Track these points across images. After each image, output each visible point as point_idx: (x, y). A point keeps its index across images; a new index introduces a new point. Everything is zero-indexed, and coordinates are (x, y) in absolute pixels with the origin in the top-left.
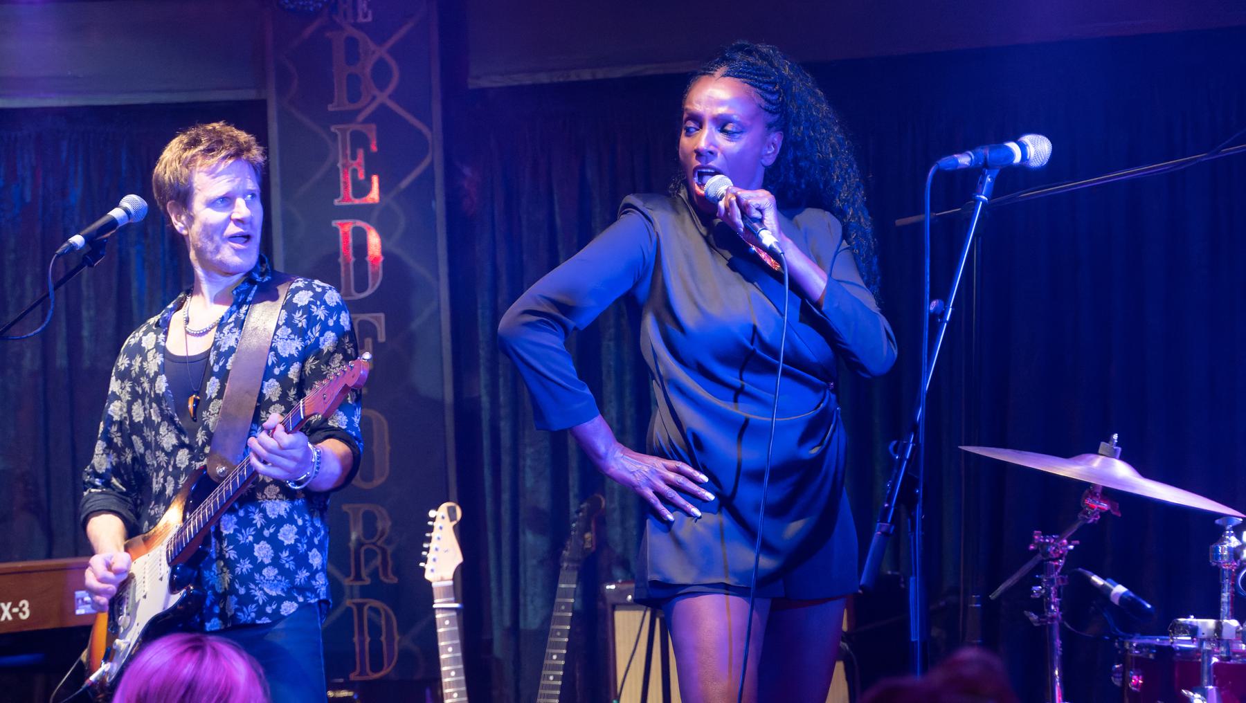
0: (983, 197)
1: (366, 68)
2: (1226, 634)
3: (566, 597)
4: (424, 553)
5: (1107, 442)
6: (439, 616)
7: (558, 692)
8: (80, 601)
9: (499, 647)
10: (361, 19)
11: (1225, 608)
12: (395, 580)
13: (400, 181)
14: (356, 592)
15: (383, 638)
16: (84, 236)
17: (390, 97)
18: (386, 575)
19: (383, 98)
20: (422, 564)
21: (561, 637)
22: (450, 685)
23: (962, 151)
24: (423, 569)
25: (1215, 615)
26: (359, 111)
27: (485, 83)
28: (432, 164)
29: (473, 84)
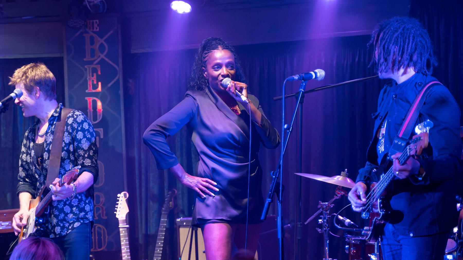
1: (97, 46)
3: (163, 223)
6: (121, 230)
7: (161, 255)
9: (141, 241)
10: (95, 30)
13: (108, 84)
15: (102, 237)
18: (103, 216)
19: (102, 56)
20: (115, 212)
22: (124, 253)
24: (116, 214)
26: (95, 61)
28: (119, 79)
29: (133, 51)
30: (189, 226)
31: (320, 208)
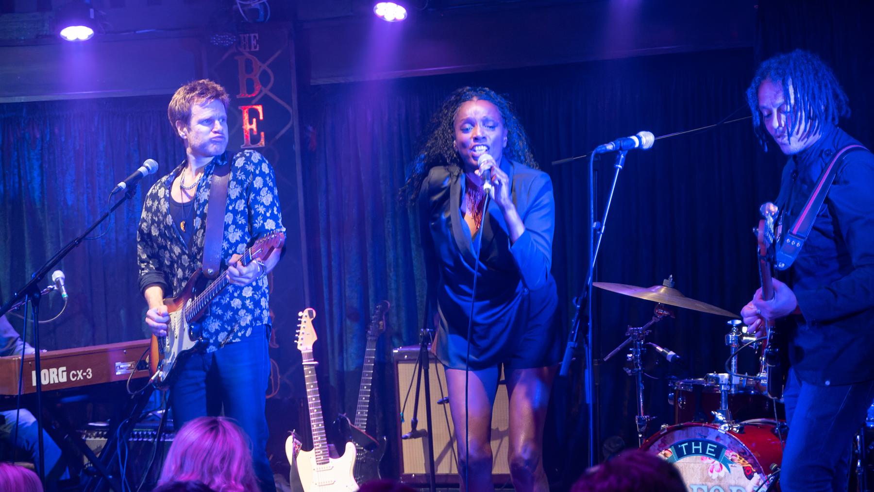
1: (256, 76)
4: (297, 335)
5: (667, 279)
6: (305, 369)
8: (118, 368)
9: (333, 382)
10: (253, 49)
11: (734, 368)
12: (277, 346)
16: (125, 183)
20: (296, 341)
21: (368, 376)
22: (312, 405)
23: (608, 142)
24: (296, 344)
26: (253, 98)
27: (321, 82)
28: (292, 128)
29: (313, 82)
30: (415, 360)
31: (629, 336)
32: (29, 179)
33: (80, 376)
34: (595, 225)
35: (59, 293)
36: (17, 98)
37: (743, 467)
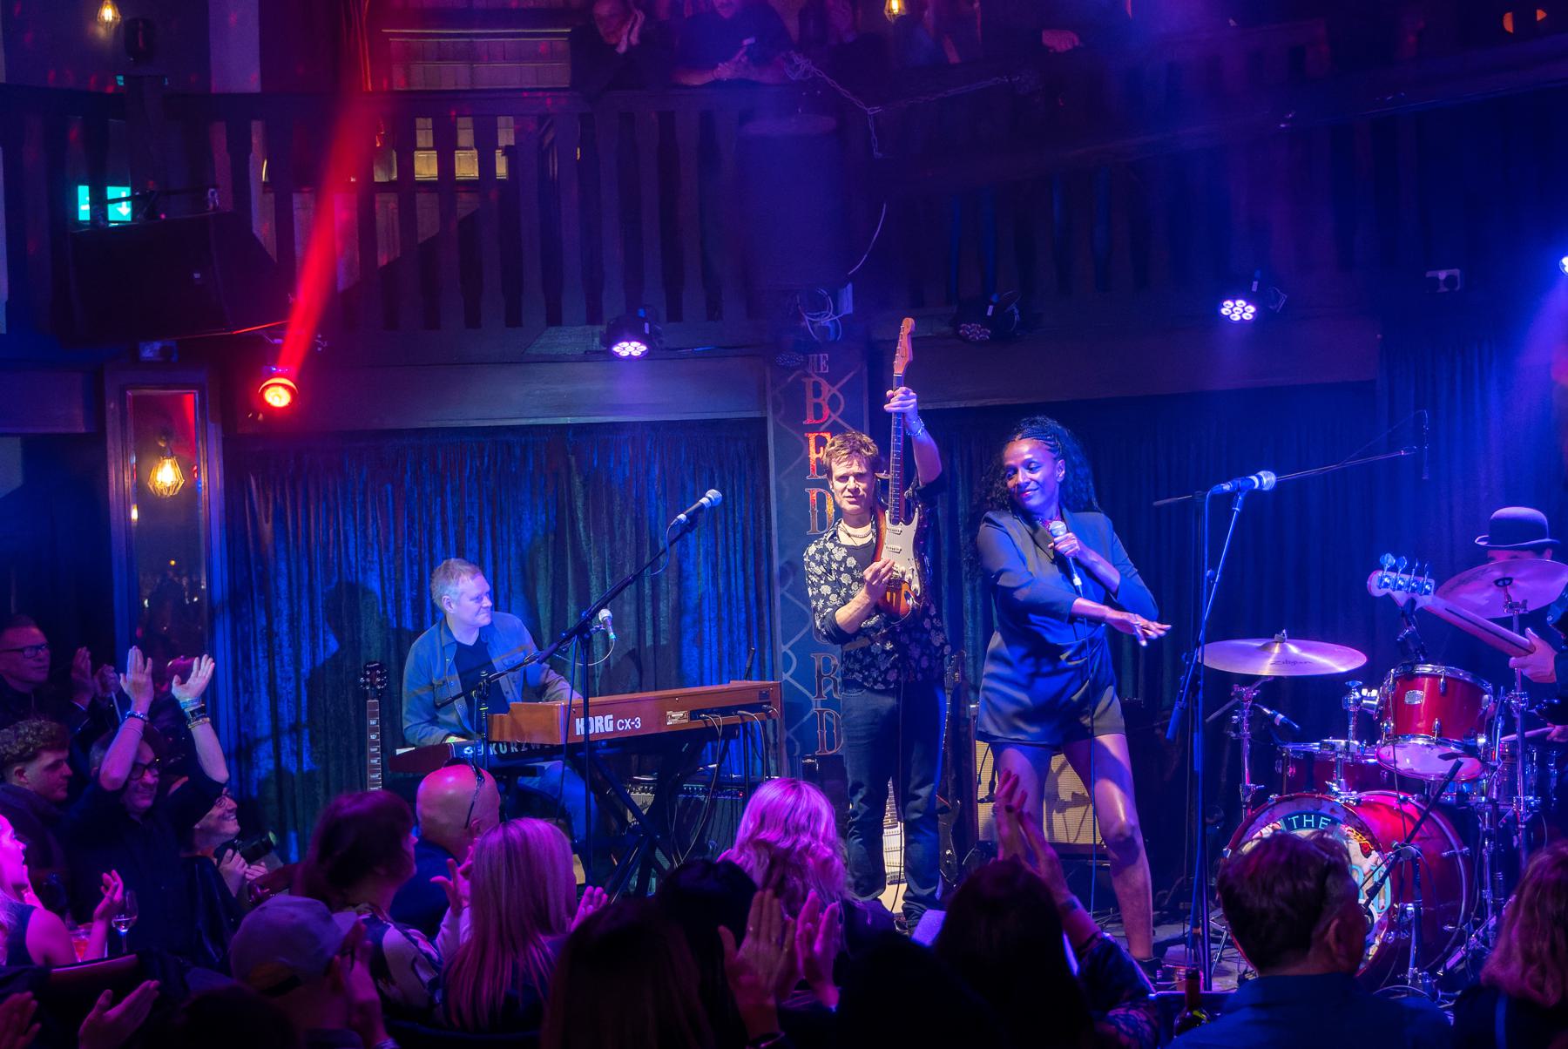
0: (1237, 509)
2: (1352, 750)
10: (822, 371)
11: (1351, 734)
14: (819, 704)
17: (839, 416)
19: (835, 417)
25: (1345, 736)
26: (820, 425)
32: (574, 507)
33: (628, 725)
34: (1208, 573)
35: (606, 635)
36: (562, 419)
37: (1360, 844)
